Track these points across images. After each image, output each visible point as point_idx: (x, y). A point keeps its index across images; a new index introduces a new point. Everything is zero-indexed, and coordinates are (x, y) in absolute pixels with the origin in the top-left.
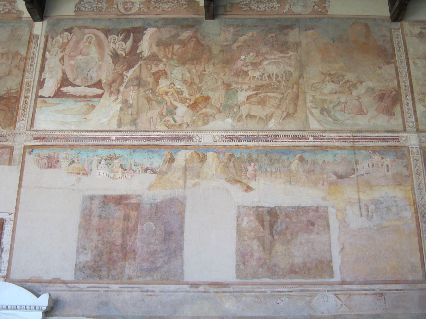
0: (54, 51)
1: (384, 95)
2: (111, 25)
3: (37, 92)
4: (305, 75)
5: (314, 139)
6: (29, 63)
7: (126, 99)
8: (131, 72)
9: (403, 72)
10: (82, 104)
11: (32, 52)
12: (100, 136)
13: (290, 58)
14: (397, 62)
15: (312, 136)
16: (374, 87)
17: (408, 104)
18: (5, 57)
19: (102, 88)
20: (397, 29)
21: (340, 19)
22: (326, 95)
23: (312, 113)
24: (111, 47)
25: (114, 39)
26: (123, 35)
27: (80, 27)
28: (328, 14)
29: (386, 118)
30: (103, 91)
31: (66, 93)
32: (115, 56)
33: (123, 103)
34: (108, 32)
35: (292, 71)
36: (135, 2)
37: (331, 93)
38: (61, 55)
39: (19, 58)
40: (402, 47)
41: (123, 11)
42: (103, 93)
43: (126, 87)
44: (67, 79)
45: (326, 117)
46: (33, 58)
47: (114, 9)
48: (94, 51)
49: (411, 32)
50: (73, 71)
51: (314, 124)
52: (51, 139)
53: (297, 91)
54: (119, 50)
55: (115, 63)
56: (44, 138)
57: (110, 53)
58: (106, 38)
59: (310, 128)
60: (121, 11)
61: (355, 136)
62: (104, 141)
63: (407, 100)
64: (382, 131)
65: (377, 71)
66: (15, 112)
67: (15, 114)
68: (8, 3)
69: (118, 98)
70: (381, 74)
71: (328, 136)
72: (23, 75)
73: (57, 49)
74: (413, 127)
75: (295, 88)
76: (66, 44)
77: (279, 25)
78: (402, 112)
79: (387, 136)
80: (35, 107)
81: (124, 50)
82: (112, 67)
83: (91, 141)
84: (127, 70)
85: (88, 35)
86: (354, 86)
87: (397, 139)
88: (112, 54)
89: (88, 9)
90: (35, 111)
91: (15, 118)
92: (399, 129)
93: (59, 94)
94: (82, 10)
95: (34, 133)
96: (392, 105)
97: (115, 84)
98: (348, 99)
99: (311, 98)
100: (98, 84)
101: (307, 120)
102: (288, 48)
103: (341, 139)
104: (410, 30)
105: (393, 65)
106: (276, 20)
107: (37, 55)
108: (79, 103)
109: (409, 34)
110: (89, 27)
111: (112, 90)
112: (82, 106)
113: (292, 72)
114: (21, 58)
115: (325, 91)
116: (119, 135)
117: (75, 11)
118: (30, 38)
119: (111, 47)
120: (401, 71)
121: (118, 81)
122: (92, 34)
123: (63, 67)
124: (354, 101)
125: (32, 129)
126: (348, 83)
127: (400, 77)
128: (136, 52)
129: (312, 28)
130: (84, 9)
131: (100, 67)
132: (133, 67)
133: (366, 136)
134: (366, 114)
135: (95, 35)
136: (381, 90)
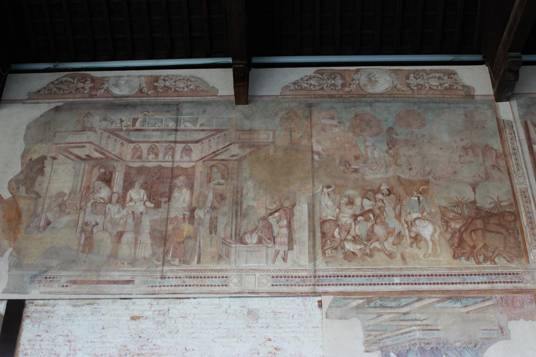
6: (512, 162)
11: (510, 145)
18: (470, 153)
39: (494, 155)
46: (515, 154)
66: (520, 236)
67: (520, 239)
68: (444, 76)
72: (511, 180)
91: (522, 245)
107: (520, 149)
114: (497, 154)
118: (499, 126)
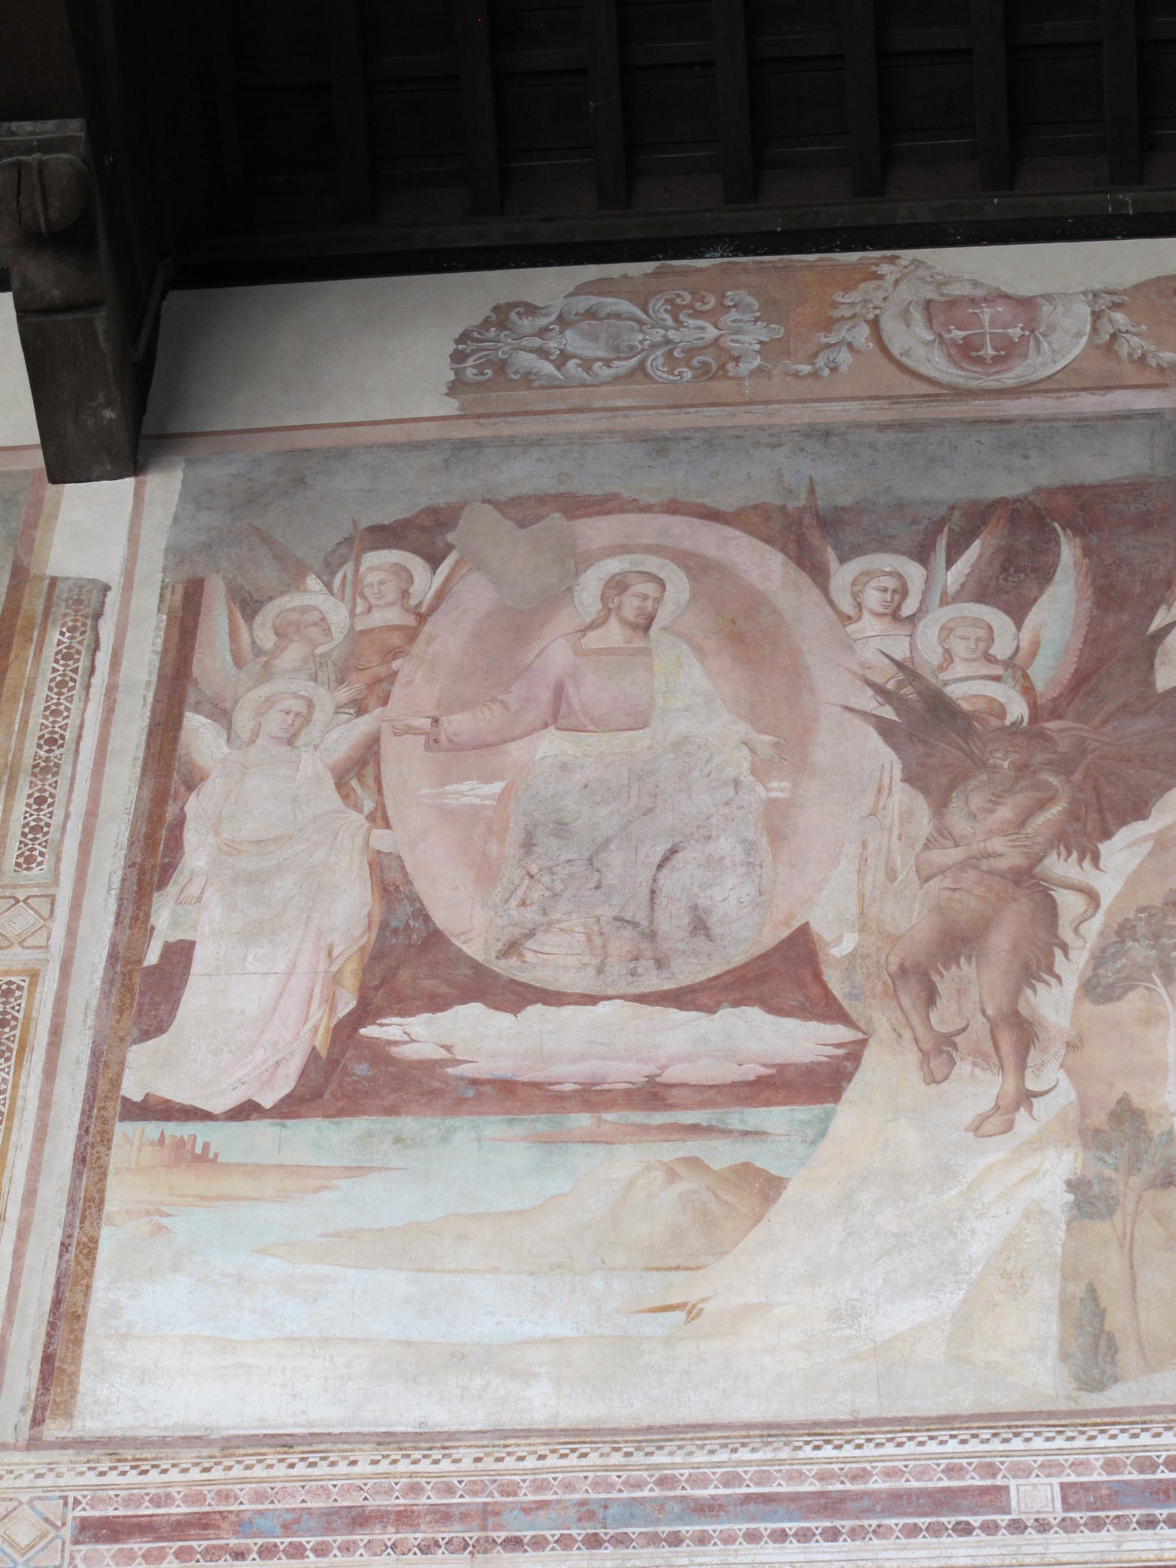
0: (270, 702)
2: (836, 481)
3: (104, 1067)
7: (1124, 1101)
8: (1124, 852)
10: (628, 1161)
12: (877, 1484)
19: (828, 1009)
24: (868, 653)
25: (890, 583)
26: (975, 549)
27: (517, 501)
30: (842, 1033)
31: (430, 1067)
32: (928, 727)
33: (1094, 1139)
34: (815, 537)
36: (1048, 297)
38: (346, 736)
41: (938, 365)
42: (854, 1053)
43: (1095, 989)
44: (435, 938)
46: (45, 769)
47: (844, 357)
48: (693, 697)
50: (486, 873)
52: (287, 1528)
54: (959, 669)
55: (934, 781)
56: (202, 1524)
57: (868, 701)
58: (804, 579)
60: (924, 369)
62: (936, 1530)
69: (1026, 1098)
73: (305, 687)
76: (396, 640)
80: (87, 1204)
81: (1016, 668)
82: (907, 816)
83: (780, 1536)
84: (1086, 832)
85: (613, 566)
88: (888, 712)
89: (587, 364)
90: (89, 1250)
93: (343, 1079)
94: (528, 379)
95: (74, 1476)
97: (967, 969)
100: (787, 974)
108: (587, 1160)
110: (613, 497)
111: (944, 1017)
112: (631, 1183)
116: (1111, 1466)
117: (453, 389)
119: (868, 653)
121: (1001, 940)
122: (655, 550)
123: (382, 840)
125: (53, 1430)
128: (1148, 679)
130: (548, 368)
131: (777, 824)
132: (1139, 812)
135: (682, 558)
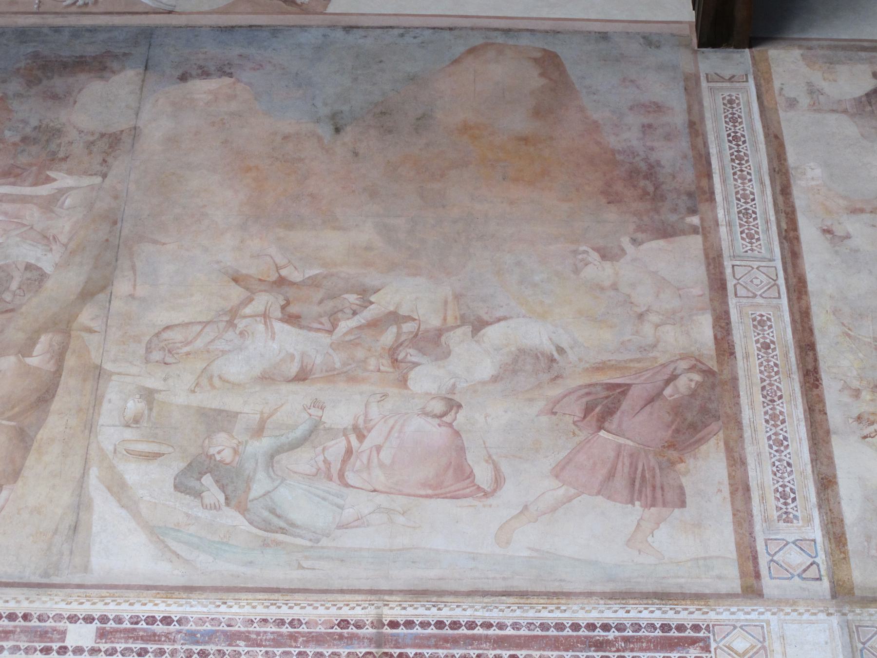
1: (619, 391)
4: (122, 287)
5: (102, 634)
9: (756, 276)
13: (49, 204)
14: (723, 230)
15: (89, 619)
16: (561, 350)
17: (780, 443)
20: (731, 79)
21: (396, 32)
22: (234, 386)
23: (118, 488)
28: (331, 9)
29: (626, 516)
35: (47, 262)
37: (267, 378)
40: (759, 157)
45: (216, 507)
49: (812, 91)
51: (120, 548)
53: (51, 367)
59: (86, 568)
61: (394, 625)
63: (774, 418)
64: (590, 594)
65: (589, 273)
70: (615, 287)
71: (202, 621)
74: (813, 572)
75: (39, 348)
77: (36, 55)
78: (740, 489)
79: (620, 628)
86: (432, 342)
87: (693, 642)
92: (706, 584)
96: (671, 445)
98: (374, 412)
99: (134, 406)
101: (75, 528)
102: (54, 159)
103: (293, 637)
104: (809, 84)
105: (695, 243)
106: (23, 34)
109: (805, 101)
113: (48, 268)
115: (235, 368)
120: (740, 272)
124: (418, 423)
126: (394, 329)
127: (732, 301)
129: (224, 70)
133: (471, 625)
134: (486, 495)
136: (600, 368)
